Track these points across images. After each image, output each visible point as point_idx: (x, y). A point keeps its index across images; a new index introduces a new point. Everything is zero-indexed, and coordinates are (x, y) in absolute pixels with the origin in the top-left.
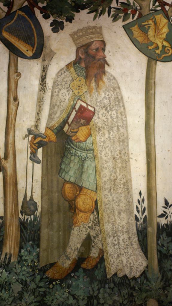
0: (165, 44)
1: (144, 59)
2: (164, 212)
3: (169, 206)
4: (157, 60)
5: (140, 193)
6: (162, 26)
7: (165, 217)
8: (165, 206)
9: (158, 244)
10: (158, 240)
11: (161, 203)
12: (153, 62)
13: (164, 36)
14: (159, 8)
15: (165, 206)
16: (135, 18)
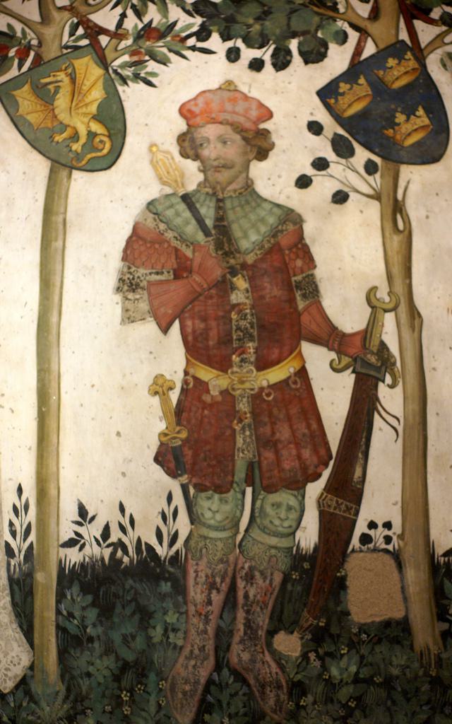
0: (96, 127)
1: (40, 167)
2: (77, 534)
3: (88, 520)
4: (72, 168)
5: (20, 490)
6: (88, 83)
7: (78, 546)
8: (80, 520)
9: (58, 612)
10: (58, 602)
11: (69, 512)
12: (64, 173)
13: (93, 109)
14: (85, 42)
15: (80, 520)
16: (25, 69)
